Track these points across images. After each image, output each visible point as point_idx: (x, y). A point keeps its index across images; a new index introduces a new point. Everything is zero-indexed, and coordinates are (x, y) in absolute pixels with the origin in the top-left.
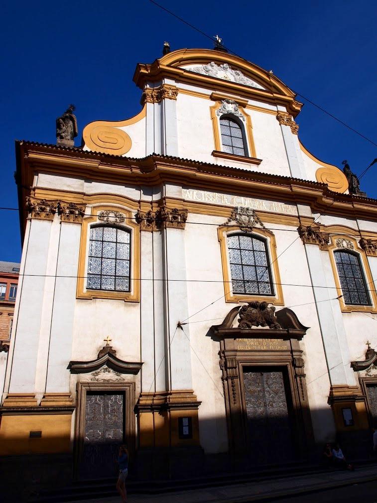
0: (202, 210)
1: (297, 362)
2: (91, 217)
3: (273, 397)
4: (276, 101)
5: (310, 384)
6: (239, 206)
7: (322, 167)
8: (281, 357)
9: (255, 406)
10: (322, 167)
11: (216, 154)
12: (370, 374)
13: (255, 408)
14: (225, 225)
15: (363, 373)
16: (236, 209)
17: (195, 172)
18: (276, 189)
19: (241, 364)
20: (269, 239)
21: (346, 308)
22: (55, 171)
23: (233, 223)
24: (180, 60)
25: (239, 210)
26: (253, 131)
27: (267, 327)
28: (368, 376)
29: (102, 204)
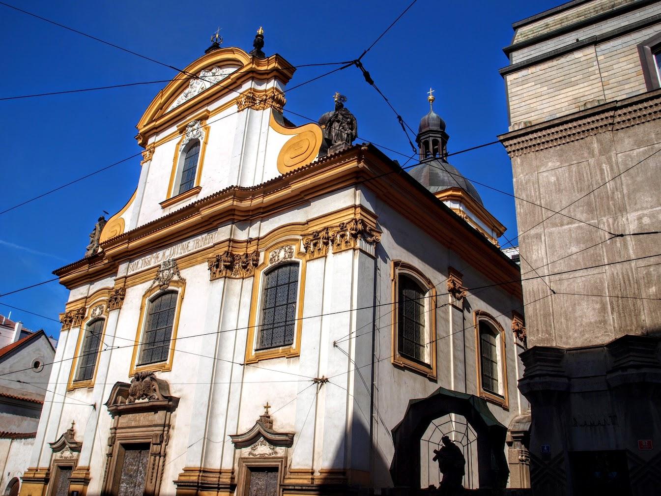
0: (137, 280)
1: (164, 438)
2: (87, 317)
3: (142, 478)
4: (239, 82)
5: (169, 465)
6: (161, 263)
7: (291, 136)
8: (147, 433)
9: (128, 486)
10: (291, 136)
11: (164, 205)
12: (254, 452)
13: (127, 488)
14: (150, 290)
15: (246, 451)
16: (159, 266)
17: (127, 245)
18: (176, 229)
19: (119, 441)
20: (180, 290)
21: (254, 357)
22: (101, 276)
23: (157, 283)
24: (161, 108)
25: (162, 266)
26: (208, 147)
27: (146, 400)
28: (251, 456)
29: (95, 301)
